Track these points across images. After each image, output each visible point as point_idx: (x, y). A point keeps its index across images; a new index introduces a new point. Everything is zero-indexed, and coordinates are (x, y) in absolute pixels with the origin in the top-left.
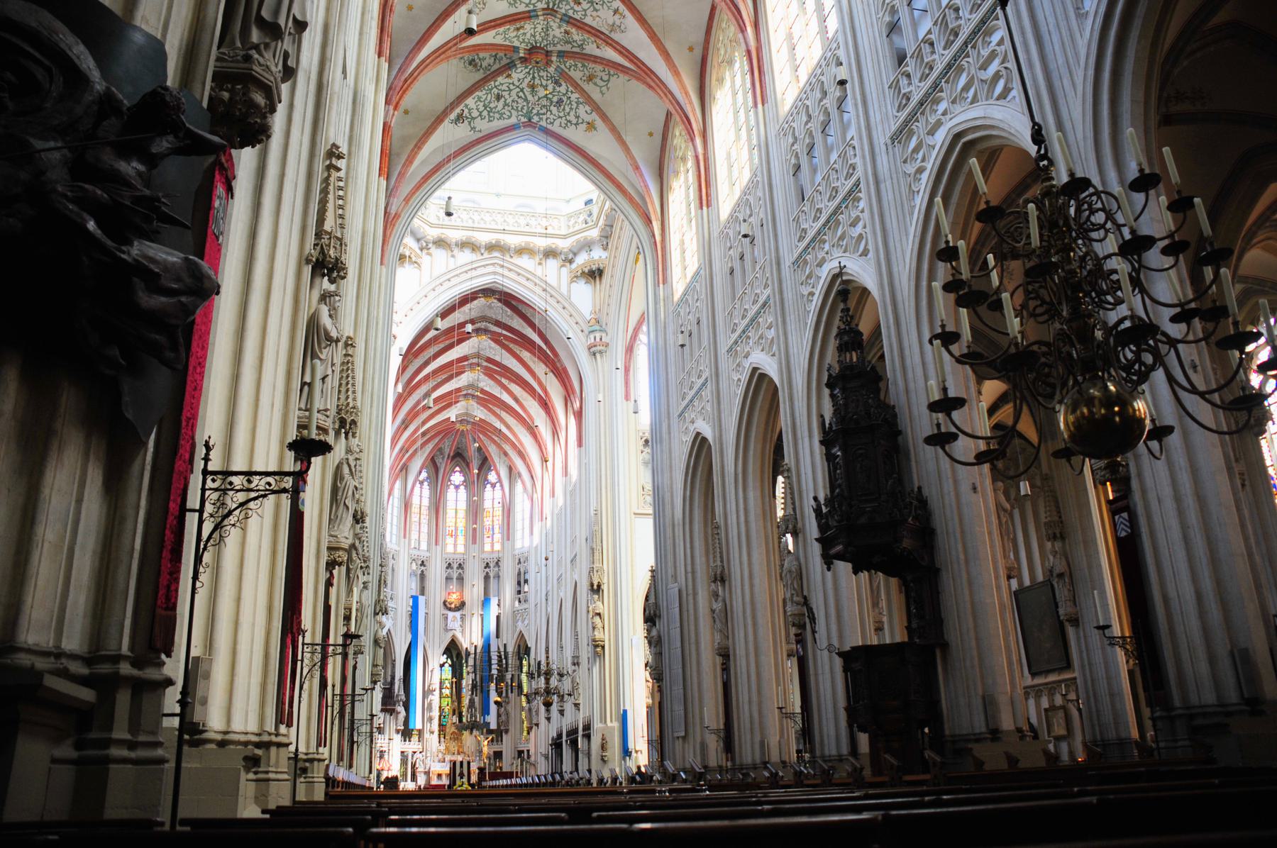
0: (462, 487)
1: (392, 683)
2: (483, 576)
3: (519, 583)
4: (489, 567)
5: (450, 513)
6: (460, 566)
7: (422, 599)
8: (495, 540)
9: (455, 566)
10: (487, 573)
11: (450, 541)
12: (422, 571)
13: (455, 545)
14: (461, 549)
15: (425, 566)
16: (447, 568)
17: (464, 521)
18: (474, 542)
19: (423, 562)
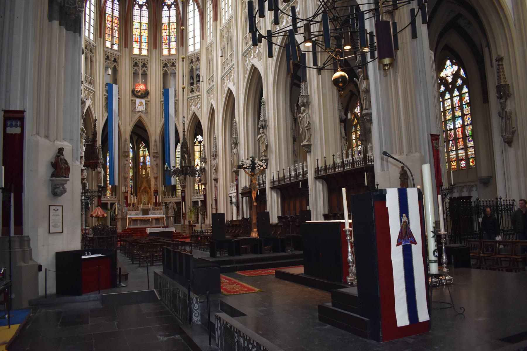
0: (145, 7)
1: (94, 140)
2: (162, 73)
3: (191, 77)
4: (167, 67)
5: (136, 25)
6: (144, 65)
7: (115, 87)
8: (171, 47)
9: (140, 65)
10: (166, 71)
11: (136, 45)
12: (115, 66)
13: (140, 49)
14: (144, 53)
15: (117, 62)
16: (134, 66)
17: (147, 32)
18: (155, 47)
19: (115, 59)
